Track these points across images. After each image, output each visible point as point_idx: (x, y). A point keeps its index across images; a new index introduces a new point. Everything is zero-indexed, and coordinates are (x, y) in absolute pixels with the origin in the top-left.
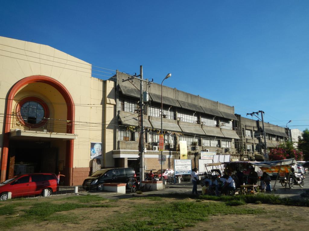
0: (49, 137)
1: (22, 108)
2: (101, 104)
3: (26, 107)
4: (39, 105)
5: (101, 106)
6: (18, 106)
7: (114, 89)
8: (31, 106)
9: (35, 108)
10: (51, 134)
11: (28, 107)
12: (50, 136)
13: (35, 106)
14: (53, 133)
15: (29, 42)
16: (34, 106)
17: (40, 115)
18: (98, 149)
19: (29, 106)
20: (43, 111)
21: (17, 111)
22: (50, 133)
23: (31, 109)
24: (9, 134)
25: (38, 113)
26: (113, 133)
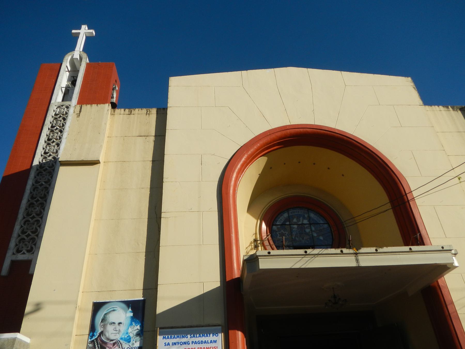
0: (354, 264)
1: (274, 227)
3: (283, 224)
4: (312, 215)
6: (264, 226)
8: (295, 220)
9: (306, 222)
10: (356, 254)
11: (288, 223)
12: (357, 261)
13: (304, 218)
14: (363, 250)
15: (248, 71)
16: (301, 218)
17: (321, 238)
19: (290, 222)
20: (326, 226)
21: (264, 235)
22: (351, 251)
24: (238, 281)
25: (315, 235)
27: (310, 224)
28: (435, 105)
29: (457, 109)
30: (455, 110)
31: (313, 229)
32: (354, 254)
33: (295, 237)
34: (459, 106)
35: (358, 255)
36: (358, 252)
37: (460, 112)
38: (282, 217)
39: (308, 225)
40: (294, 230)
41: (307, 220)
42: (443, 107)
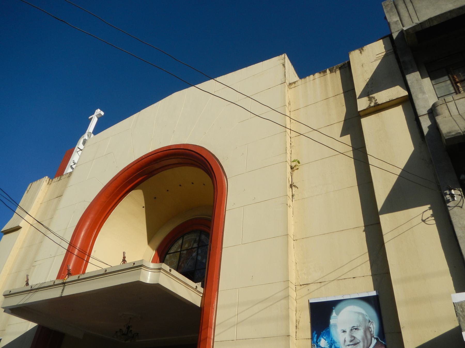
2: (343, 134)
5: (347, 138)
7: (392, 58)
18: (359, 335)
23: (185, 252)
25: (199, 258)
26: (432, 221)
27: (198, 248)
28: (309, 75)
29: (336, 69)
30: (334, 71)
31: (200, 252)
32: (63, 284)
33: (181, 264)
34: (339, 65)
35: (66, 284)
36: (64, 281)
37: (338, 72)
38: (177, 244)
39: (196, 249)
40: (183, 256)
41: (197, 243)
42: (320, 73)
